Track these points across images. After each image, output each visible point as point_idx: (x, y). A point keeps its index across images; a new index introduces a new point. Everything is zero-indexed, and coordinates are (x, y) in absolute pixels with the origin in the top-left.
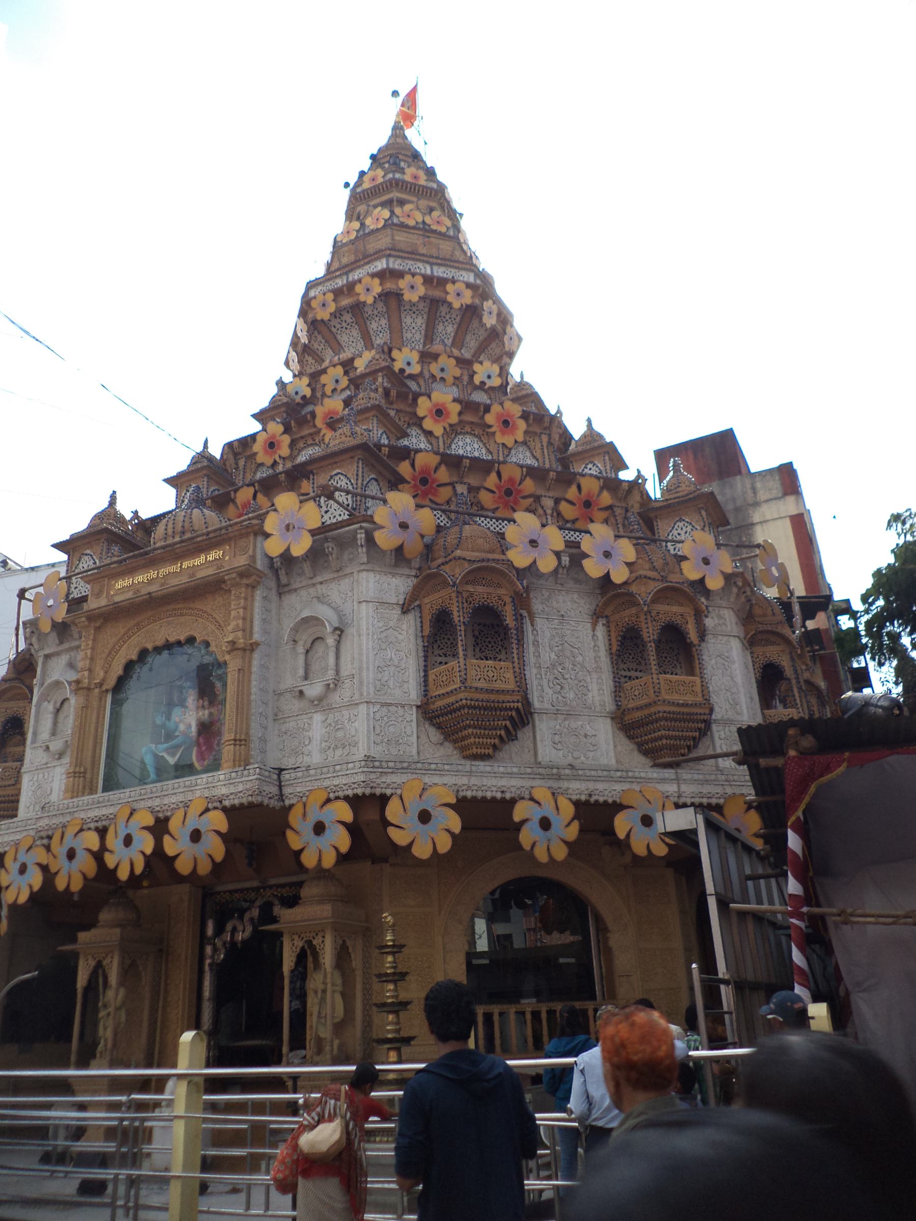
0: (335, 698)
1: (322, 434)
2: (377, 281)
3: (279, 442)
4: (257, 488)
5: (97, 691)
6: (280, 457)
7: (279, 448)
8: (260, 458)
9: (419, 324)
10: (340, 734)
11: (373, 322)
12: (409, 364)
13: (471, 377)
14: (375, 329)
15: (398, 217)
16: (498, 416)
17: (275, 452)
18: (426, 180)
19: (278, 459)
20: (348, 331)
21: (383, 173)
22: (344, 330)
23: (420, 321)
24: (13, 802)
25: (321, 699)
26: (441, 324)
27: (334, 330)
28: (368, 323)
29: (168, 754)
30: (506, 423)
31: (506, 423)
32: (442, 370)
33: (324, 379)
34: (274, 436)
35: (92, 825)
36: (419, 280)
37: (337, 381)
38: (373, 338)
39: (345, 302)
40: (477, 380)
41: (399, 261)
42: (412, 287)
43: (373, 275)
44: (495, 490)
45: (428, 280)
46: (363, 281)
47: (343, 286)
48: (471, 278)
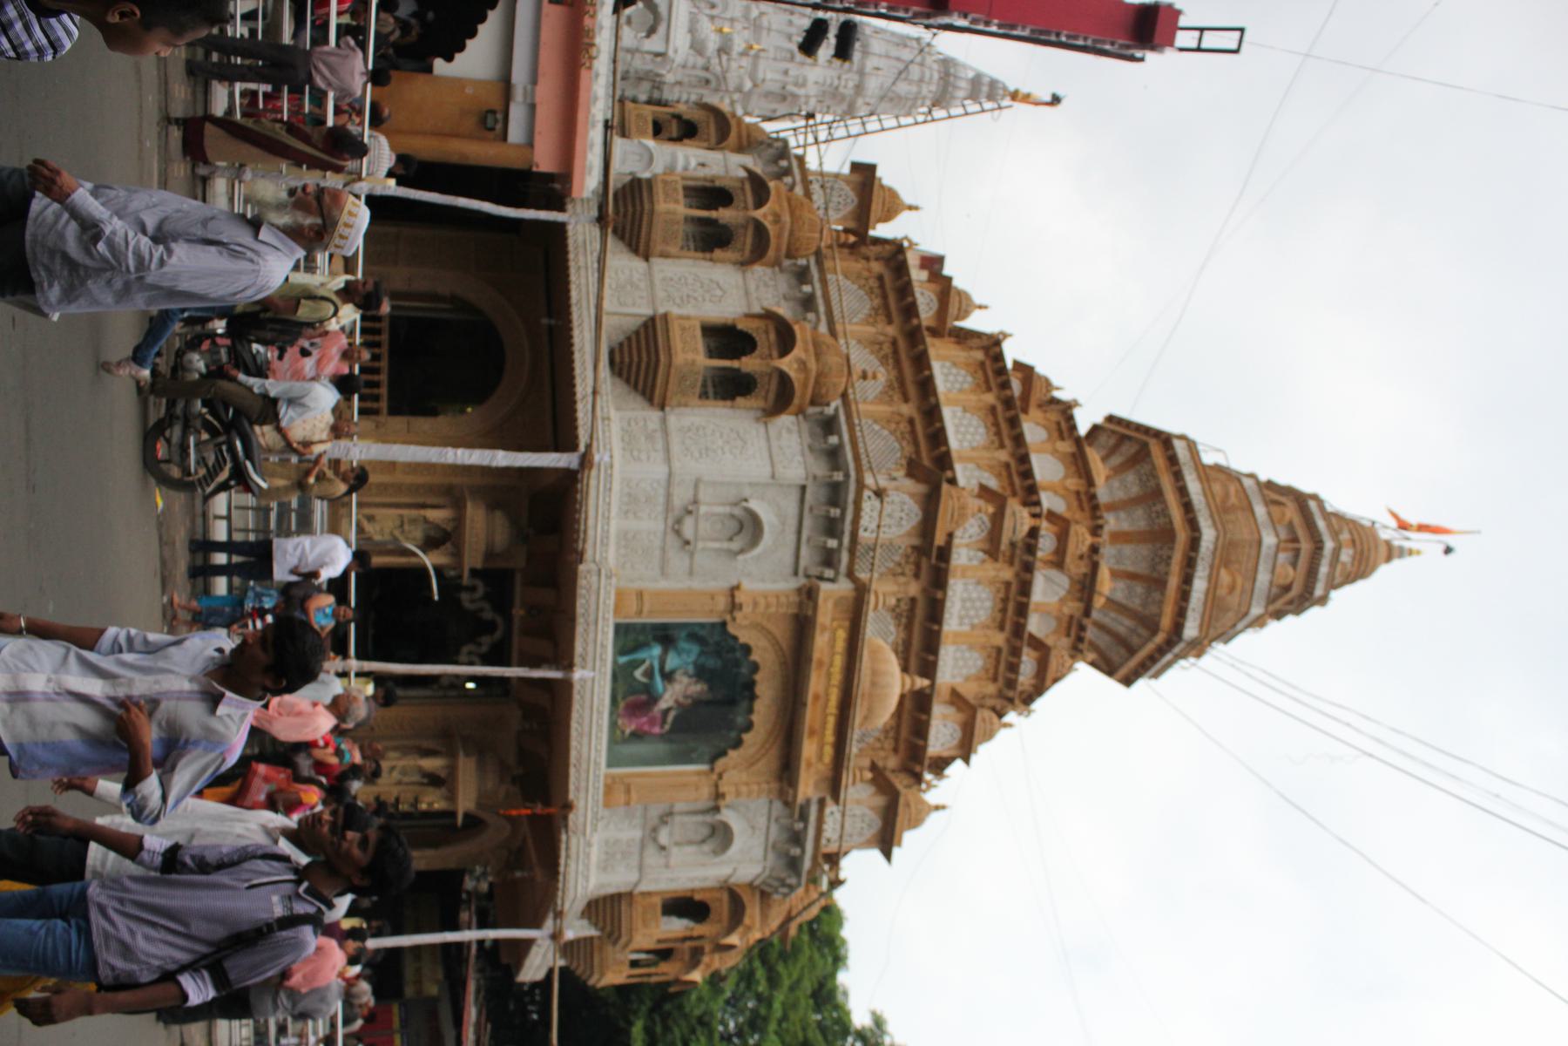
0: (651, 850)
10: (619, 856)
23: (1121, 630)
25: (655, 840)
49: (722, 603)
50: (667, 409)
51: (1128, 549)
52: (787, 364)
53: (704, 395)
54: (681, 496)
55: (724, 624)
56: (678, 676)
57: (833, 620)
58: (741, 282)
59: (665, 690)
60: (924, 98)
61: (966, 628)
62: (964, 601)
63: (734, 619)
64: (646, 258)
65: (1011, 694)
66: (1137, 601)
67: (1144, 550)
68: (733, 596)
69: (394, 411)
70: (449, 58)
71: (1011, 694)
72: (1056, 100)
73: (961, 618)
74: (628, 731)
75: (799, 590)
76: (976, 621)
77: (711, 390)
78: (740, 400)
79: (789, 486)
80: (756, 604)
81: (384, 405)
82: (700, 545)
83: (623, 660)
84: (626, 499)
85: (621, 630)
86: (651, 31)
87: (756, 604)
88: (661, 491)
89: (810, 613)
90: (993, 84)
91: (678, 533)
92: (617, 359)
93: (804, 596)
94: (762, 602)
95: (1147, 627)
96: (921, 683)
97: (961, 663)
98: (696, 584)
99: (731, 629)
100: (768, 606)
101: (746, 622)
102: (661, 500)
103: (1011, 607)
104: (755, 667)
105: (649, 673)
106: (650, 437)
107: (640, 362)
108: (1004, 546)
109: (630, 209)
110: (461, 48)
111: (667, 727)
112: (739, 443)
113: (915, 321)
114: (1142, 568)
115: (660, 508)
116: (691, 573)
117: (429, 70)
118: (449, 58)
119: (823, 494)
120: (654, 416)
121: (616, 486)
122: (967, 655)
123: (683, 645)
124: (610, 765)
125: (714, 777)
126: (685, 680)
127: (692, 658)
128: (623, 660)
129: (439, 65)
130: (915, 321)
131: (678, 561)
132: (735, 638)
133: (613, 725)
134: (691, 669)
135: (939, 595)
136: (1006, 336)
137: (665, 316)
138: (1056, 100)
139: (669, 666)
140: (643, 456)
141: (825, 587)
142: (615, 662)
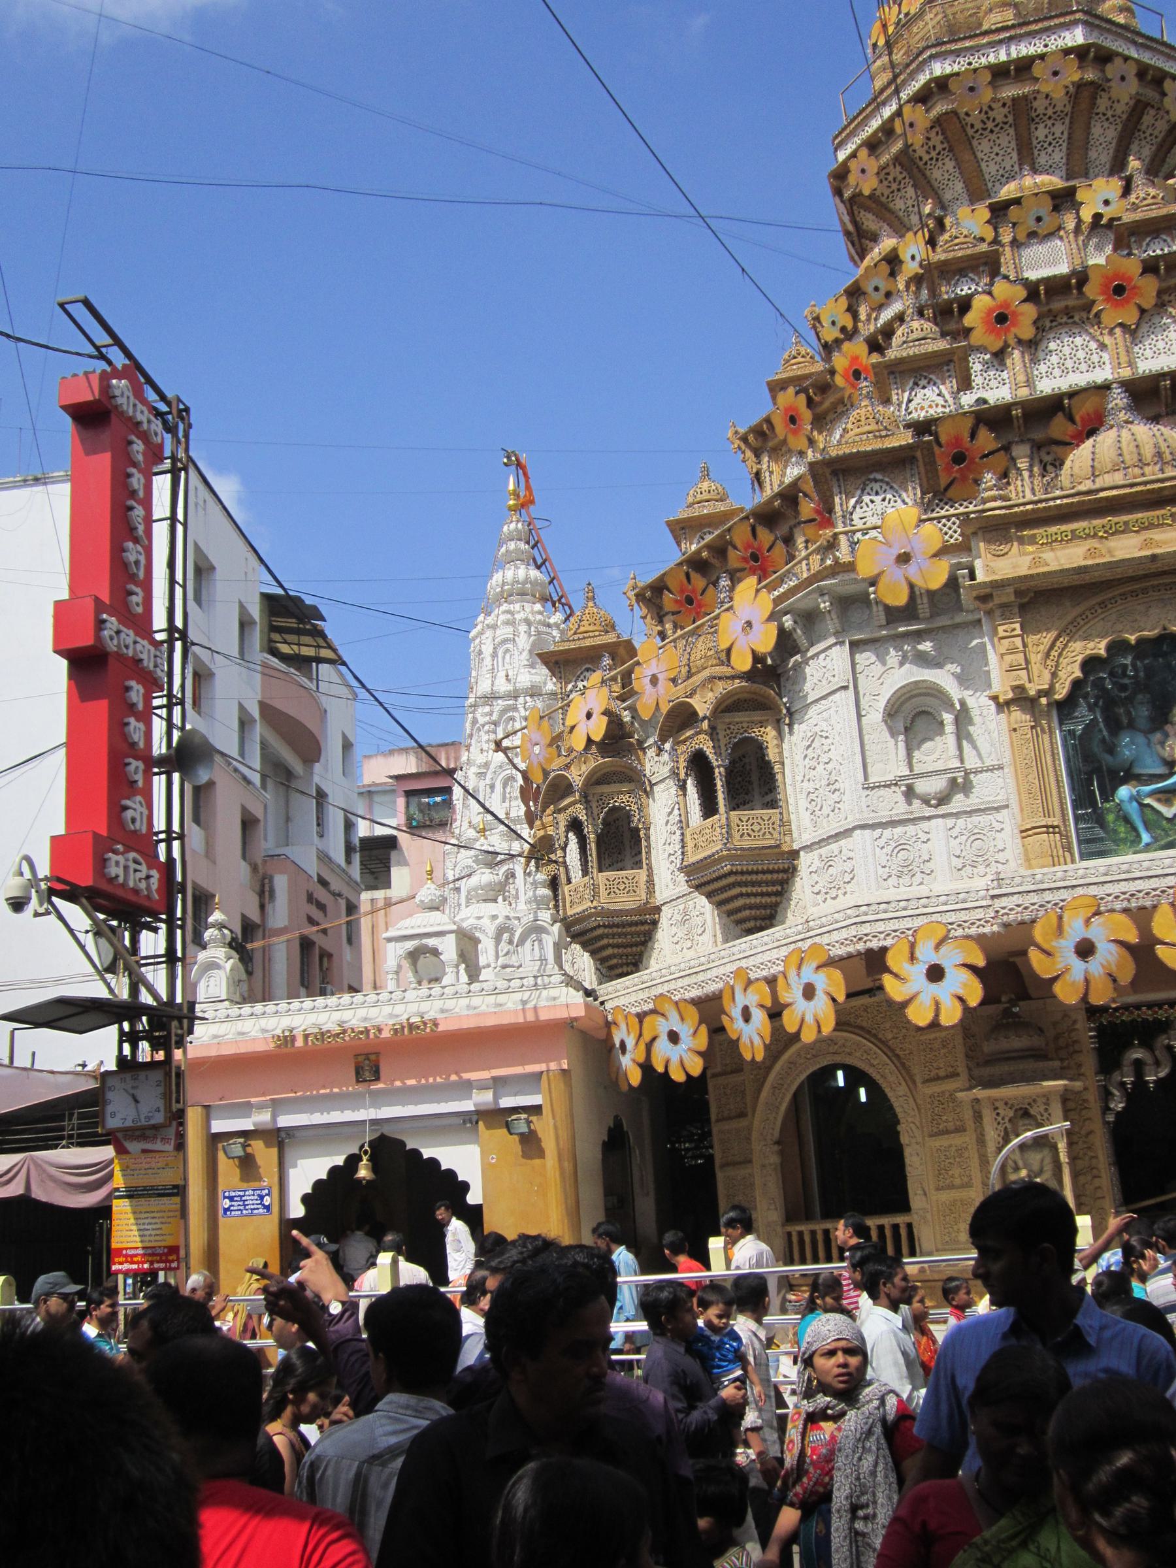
1: (1094, 311)
9: (1108, 139)
11: (1041, 126)
12: (1107, 203)
14: (1042, 138)
17: (1008, 330)
20: (993, 137)
22: (986, 133)
23: (1112, 133)
24: (785, 871)
26: (1137, 142)
27: (970, 132)
28: (1033, 126)
29: (1159, 800)
34: (1006, 304)
35: (1118, 906)
36: (1131, 70)
37: (1039, 219)
38: (1036, 153)
39: (1010, 91)
43: (1067, 52)
45: (1143, 72)
47: (1009, 63)
49: (1019, 716)
50: (795, 847)
51: (990, 169)
52: (702, 705)
53: (773, 804)
54: (892, 804)
55: (1060, 705)
58: (662, 786)
61: (1106, 356)
62: (1065, 372)
63: (1047, 693)
64: (658, 909)
66: (1059, 129)
67: (983, 147)
68: (1008, 703)
69: (905, 1207)
70: (465, 1187)
73: (1092, 367)
75: (989, 613)
76: (1093, 345)
77: (768, 798)
78: (772, 754)
79: (854, 665)
80: (1012, 669)
81: (901, 1219)
82: (956, 763)
83: (1146, 838)
84: (906, 879)
85: (1093, 848)
86: (435, 952)
87: (1012, 669)
88: (888, 833)
89: (1010, 590)
91: (943, 800)
92: (750, 924)
93: (990, 605)
94: (1008, 658)
95: (1094, 98)
96: (1118, 398)
98: (1007, 759)
99: (1061, 692)
100: (1013, 651)
101: (1047, 676)
102: (899, 830)
103: (1058, 305)
104: (1118, 647)
106: (828, 863)
107: (752, 892)
108: (942, 345)
109: (605, 941)
110: (451, 1174)
112: (816, 744)
114: (1007, 140)
115: (911, 829)
116: (1001, 768)
117: (478, 1209)
118: (465, 1187)
119: (856, 615)
120: (805, 861)
121: (891, 894)
127: (1141, 739)
129: (473, 1198)
130: (704, 554)
131: (987, 789)
132: (1077, 685)
134: (1158, 736)
137: (689, 870)
140: (848, 866)
141: (981, 577)
142: (1148, 848)
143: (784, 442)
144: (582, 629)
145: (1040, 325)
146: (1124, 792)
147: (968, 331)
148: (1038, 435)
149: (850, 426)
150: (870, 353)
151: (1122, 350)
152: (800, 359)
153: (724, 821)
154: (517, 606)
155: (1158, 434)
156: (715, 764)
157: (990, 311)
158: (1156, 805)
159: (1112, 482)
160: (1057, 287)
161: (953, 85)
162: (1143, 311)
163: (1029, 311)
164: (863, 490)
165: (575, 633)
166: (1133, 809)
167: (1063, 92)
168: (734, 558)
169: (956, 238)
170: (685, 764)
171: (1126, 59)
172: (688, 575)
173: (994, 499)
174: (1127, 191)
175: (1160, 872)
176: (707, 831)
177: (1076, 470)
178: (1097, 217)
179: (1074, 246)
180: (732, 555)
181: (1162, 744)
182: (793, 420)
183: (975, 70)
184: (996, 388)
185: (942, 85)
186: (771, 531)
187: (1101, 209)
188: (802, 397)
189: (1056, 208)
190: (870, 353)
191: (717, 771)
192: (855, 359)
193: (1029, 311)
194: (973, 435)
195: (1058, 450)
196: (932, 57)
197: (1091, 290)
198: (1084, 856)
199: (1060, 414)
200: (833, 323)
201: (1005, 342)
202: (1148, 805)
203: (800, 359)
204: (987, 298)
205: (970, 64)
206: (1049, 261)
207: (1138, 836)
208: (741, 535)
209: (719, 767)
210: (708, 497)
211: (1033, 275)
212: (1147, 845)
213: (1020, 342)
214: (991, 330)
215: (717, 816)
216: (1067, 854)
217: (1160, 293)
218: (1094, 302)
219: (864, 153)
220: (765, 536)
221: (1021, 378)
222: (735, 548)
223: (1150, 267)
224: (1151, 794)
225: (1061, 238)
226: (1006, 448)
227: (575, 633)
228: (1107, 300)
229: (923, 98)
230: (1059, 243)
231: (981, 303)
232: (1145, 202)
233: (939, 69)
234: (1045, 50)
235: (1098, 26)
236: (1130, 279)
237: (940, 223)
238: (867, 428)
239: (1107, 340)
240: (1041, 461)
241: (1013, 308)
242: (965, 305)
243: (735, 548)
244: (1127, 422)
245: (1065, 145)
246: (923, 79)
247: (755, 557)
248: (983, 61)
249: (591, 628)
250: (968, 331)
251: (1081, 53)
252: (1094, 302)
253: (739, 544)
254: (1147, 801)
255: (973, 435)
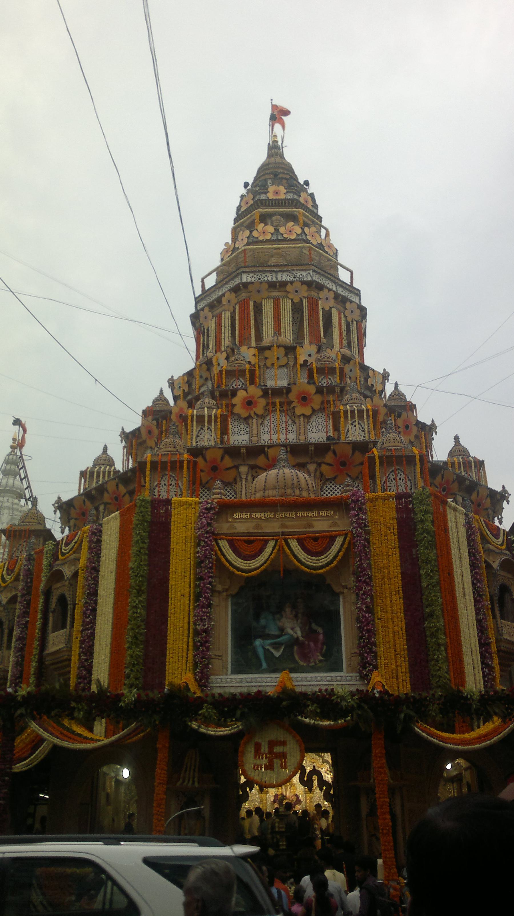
1: (292, 406)
2: (305, 287)
3: (256, 402)
4: (288, 449)
5: (225, 594)
6: (255, 413)
7: (255, 406)
8: (236, 410)
13: (366, 380)
15: (306, 235)
16: (405, 421)
17: (252, 409)
18: (312, 206)
19: (253, 415)
21: (285, 191)
29: (273, 648)
30: (407, 427)
31: (407, 427)
32: (351, 371)
33: (267, 353)
34: (253, 397)
36: (332, 295)
37: (278, 358)
40: (370, 382)
41: (318, 276)
42: (327, 299)
43: (303, 283)
44: (439, 486)
46: (294, 284)
48: (358, 302)
56: (280, 624)
57: (227, 522)
59: (289, 634)
60: (13, 504)
65: (338, 389)
71: (338, 389)
72: (17, 422)
74: (321, 658)
76: (290, 422)
83: (264, 665)
90: (7, 462)
97: (320, 427)
105: (277, 646)
111: (320, 630)
113: (93, 492)
122: (314, 424)
123: (263, 622)
124: (342, 671)
125: (346, 591)
126: (284, 620)
128: (264, 665)
133: (315, 669)
134: (278, 616)
135: (243, 450)
136: (123, 431)
138: (17, 422)
139: (277, 633)
143: (145, 442)
144: (27, 520)
145: (267, 408)
146: (258, 642)
147: (233, 406)
148: (251, 462)
149: (161, 447)
150: (188, 408)
151: (302, 427)
152: (161, 402)
153: (68, 632)
154: (5, 499)
155: (295, 475)
156: (69, 603)
157: (245, 398)
158: (273, 651)
159: (272, 494)
160: (277, 392)
161: (250, 287)
162: (314, 411)
163: (262, 402)
164: (162, 478)
165: (23, 522)
166: (260, 652)
167: (299, 300)
168: (106, 497)
169: (237, 360)
170: (56, 601)
171: (330, 290)
172: (84, 501)
173: (219, 494)
174: (319, 351)
175: (264, 684)
176: (60, 637)
177: (257, 486)
178: (306, 361)
179: (292, 373)
180: (106, 495)
181: (279, 620)
182: (150, 432)
183: (261, 283)
184: (239, 437)
185: (246, 285)
186: (125, 487)
187: (307, 358)
188: (155, 422)
189: (286, 355)
190: (188, 408)
191: (69, 606)
192: (181, 409)
193: (262, 402)
194: (222, 458)
195: (258, 470)
196: (244, 272)
197: (292, 396)
198: (233, 673)
199: (263, 455)
200: (180, 387)
201: (250, 414)
202: (268, 649)
203: (161, 402)
204: (245, 392)
205: (259, 279)
206: (277, 379)
207: (261, 665)
208: (111, 487)
209: (70, 604)
210: (104, 463)
211: (270, 384)
212: (264, 670)
213: (257, 415)
214: (244, 407)
215: (65, 630)
216: (225, 670)
217: (322, 403)
218: (292, 402)
219: (207, 309)
220: (122, 489)
221: (255, 432)
222: (108, 493)
223: (319, 391)
224: (271, 645)
225: (287, 368)
226: (236, 467)
227: (23, 522)
228: (298, 402)
229: (236, 290)
230: (286, 370)
231: (241, 394)
232: (324, 360)
233: (246, 278)
234: (294, 279)
235: (319, 273)
236: (310, 395)
237: (233, 350)
238: (170, 449)
239: (297, 421)
240: (252, 475)
241: (255, 399)
242: (234, 393)
243: (108, 493)
244: (284, 466)
245: (298, 323)
246: (237, 281)
247: (116, 499)
248: (266, 279)
249: (32, 520)
250: (233, 406)
251: (309, 284)
252: (292, 402)
253: (110, 491)
254: (267, 648)
255: (222, 458)
